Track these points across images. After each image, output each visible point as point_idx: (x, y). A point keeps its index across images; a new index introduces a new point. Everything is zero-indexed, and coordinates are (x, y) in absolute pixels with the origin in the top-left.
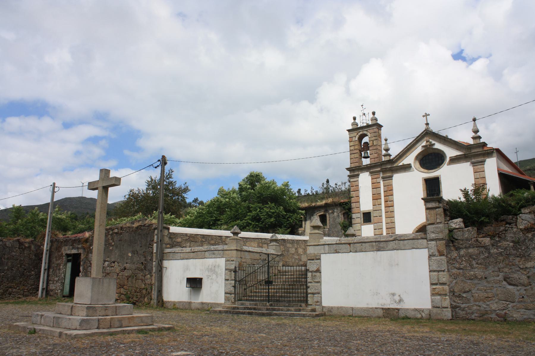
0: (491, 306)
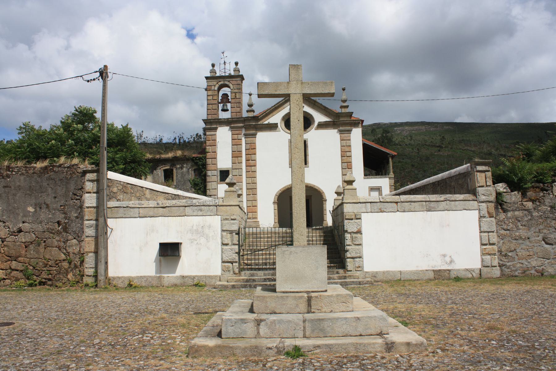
0: (532, 263)
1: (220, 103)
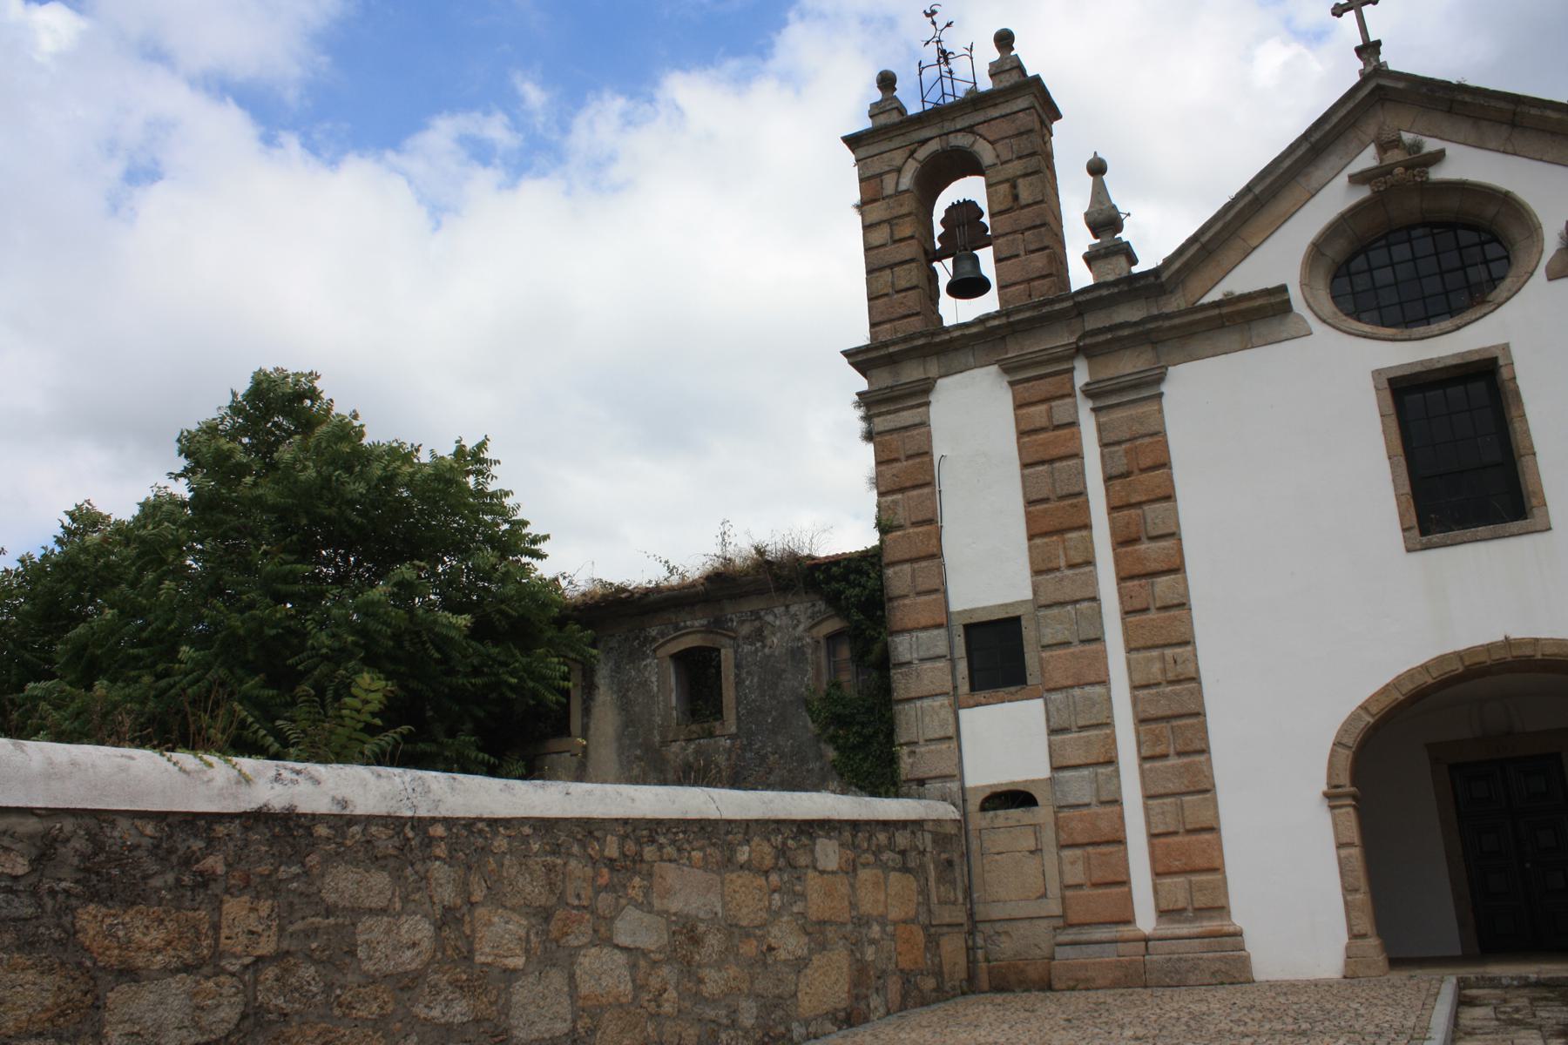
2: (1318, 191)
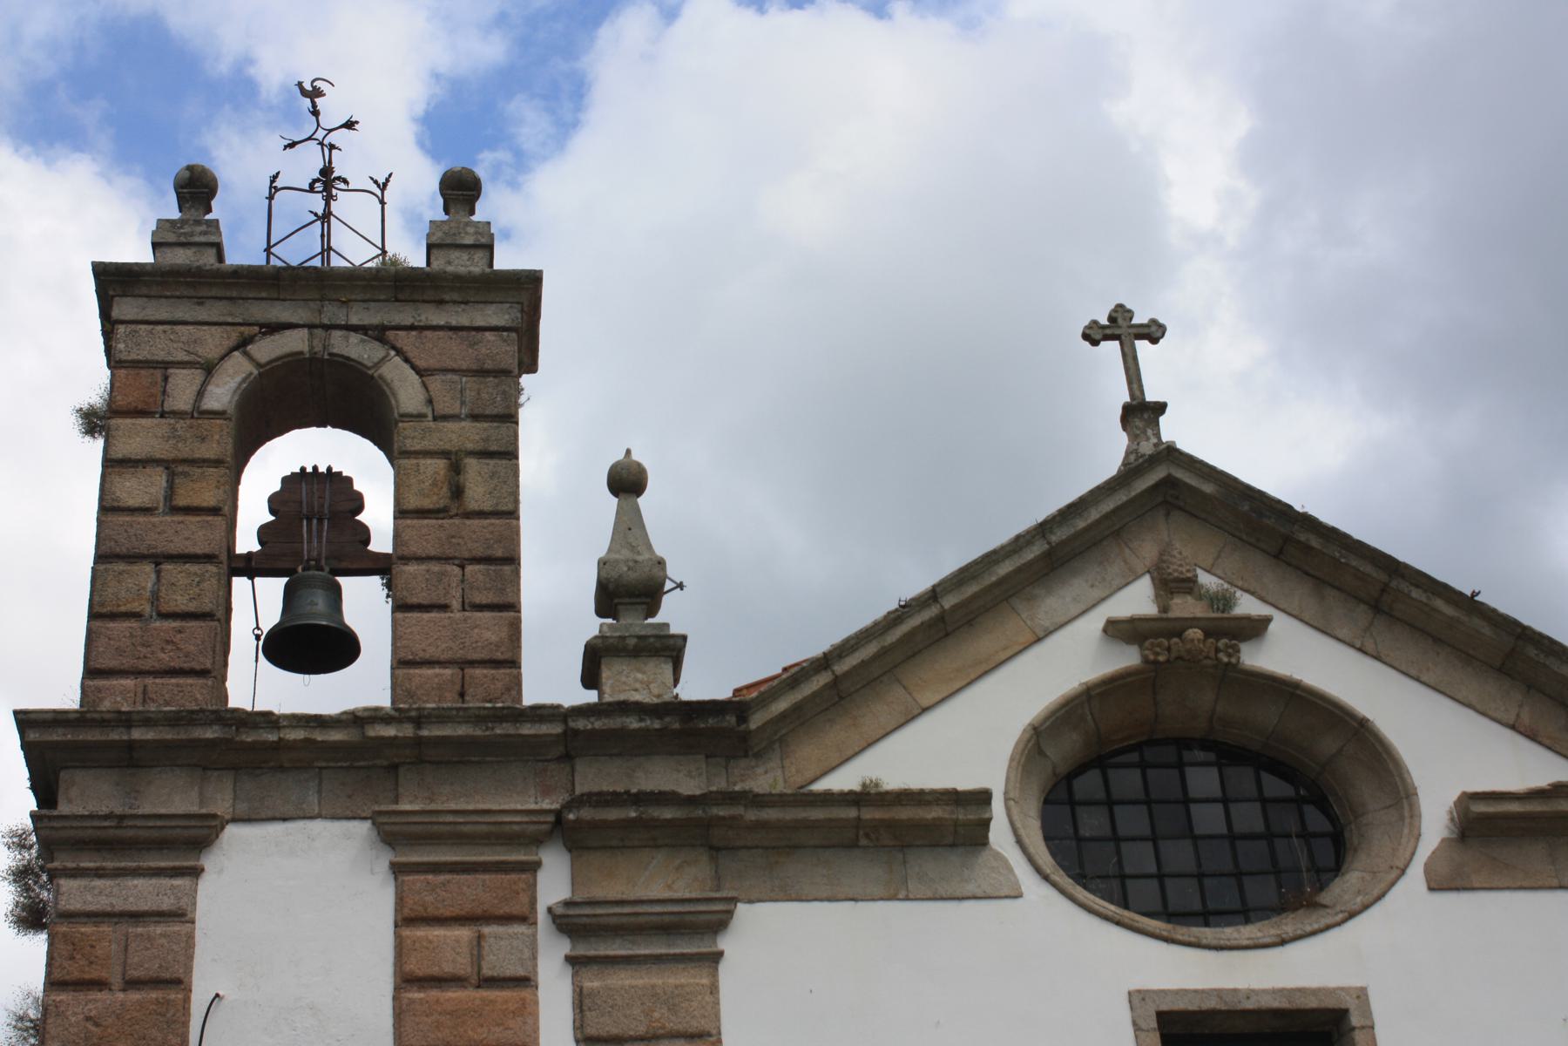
1: (251, 567)
2: (1049, 633)
